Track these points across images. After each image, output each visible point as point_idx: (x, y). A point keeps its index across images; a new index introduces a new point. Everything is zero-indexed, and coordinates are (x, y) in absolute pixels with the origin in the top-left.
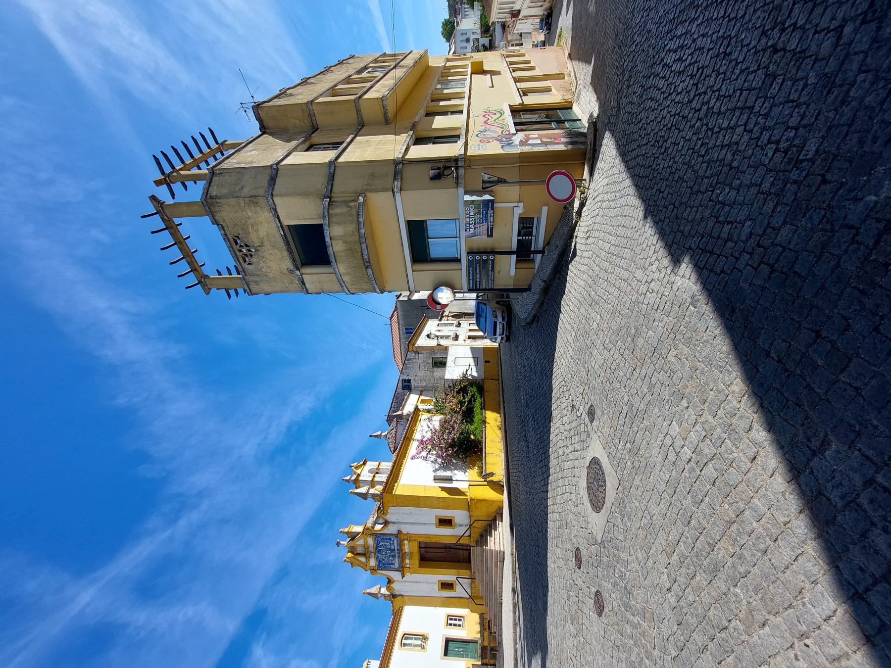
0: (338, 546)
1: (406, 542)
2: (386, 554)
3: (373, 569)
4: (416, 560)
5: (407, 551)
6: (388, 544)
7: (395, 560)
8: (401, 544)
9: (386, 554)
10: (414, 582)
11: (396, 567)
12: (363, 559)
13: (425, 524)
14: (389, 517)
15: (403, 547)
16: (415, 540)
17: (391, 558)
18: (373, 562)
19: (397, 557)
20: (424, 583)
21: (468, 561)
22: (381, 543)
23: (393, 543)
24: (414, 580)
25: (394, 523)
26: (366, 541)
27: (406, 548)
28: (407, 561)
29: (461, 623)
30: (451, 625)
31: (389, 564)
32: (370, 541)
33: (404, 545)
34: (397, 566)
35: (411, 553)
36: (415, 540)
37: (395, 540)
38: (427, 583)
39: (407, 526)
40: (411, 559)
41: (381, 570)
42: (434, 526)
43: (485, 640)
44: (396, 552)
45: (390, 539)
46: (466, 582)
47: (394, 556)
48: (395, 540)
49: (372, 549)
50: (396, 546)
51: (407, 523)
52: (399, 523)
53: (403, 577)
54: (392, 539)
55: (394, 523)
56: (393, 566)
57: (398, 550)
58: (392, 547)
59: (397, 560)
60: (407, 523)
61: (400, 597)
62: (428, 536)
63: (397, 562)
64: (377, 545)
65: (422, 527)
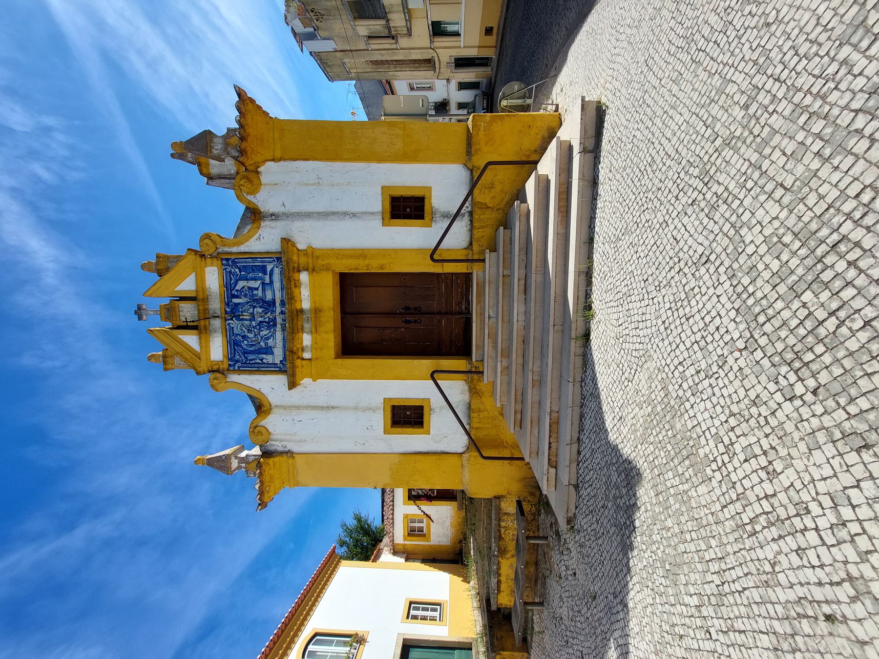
0: (140, 318)
1: (304, 277)
2: (253, 318)
3: (218, 371)
4: (330, 339)
5: (306, 305)
6: (256, 284)
7: (273, 335)
8: (290, 285)
9: (253, 318)
10: (322, 408)
11: (277, 361)
12: (191, 339)
13: (354, 215)
14: (265, 201)
15: (296, 291)
16: (327, 268)
17: (264, 332)
18: (217, 350)
19: (279, 326)
20: (346, 408)
21: (463, 349)
22: (241, 284)
23: (271, 282)
24: (322, 402)
25: (275, 216)
26: (201, 280)
27: (305, 299)
28: (307, 339)
29: (437, 614)
30: (415, 617)
31: (260, 351)
32: (213, 278)
33: (298, 285)
34: (278, 355)
35: (317, 311)
36: (327, 268)
37: (277, 271)
38: (356, 408)
39: (307, 224)
40: (315, 331)
41: (240, 371)
42: (377, 222)
43: (503, 587)
44: (278, 309)
45: (263, 269)
46: (457, 389)
47: (272, 324)
48: (277, 271)
49: (216, 305)
50: (276, 293)
51: (309, 215)
52: (287, 216)
53: (292, 385)
54: (269, 268)
55: (275, 216)
56: (269, 359)
57: (283, 303)
58: (269, 296)
59: (279, 335)
60: (309, 215)
61: (284, 458)
62: (362, 254)
63: (278, 341)
64: (229, 288)
65: (347, 224)
